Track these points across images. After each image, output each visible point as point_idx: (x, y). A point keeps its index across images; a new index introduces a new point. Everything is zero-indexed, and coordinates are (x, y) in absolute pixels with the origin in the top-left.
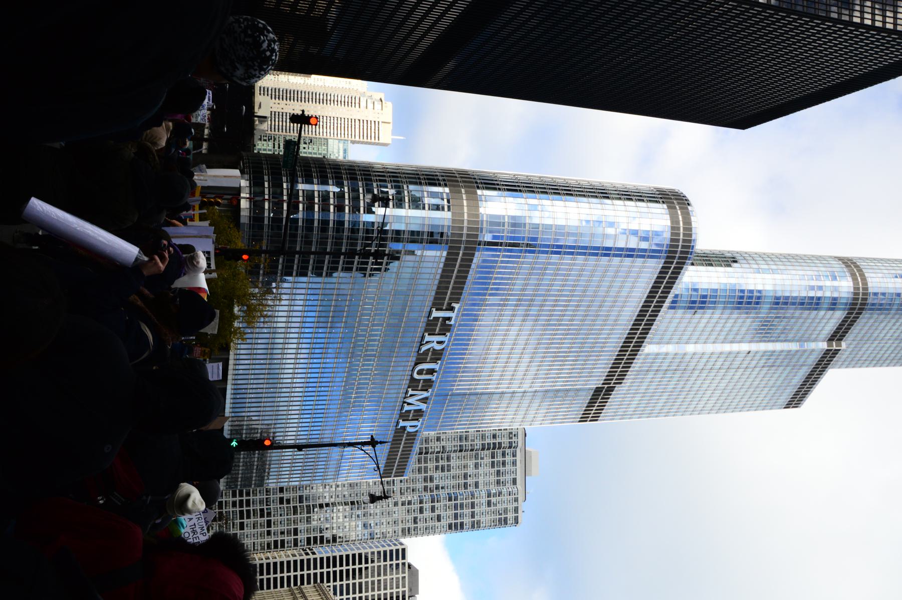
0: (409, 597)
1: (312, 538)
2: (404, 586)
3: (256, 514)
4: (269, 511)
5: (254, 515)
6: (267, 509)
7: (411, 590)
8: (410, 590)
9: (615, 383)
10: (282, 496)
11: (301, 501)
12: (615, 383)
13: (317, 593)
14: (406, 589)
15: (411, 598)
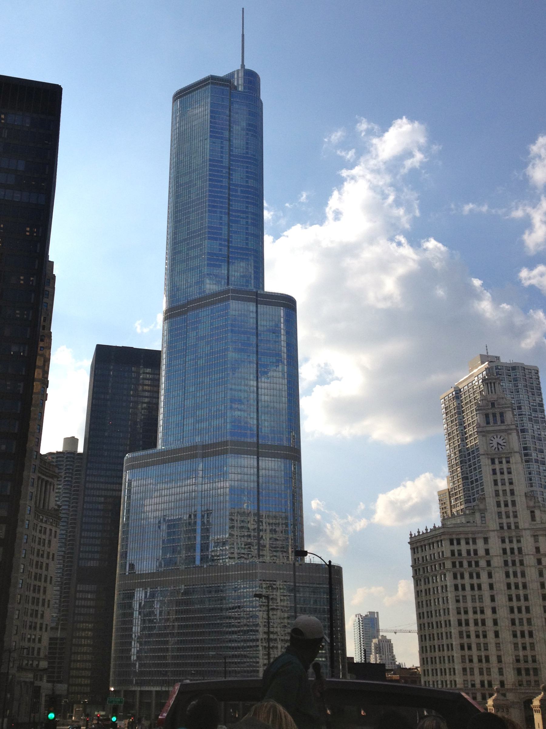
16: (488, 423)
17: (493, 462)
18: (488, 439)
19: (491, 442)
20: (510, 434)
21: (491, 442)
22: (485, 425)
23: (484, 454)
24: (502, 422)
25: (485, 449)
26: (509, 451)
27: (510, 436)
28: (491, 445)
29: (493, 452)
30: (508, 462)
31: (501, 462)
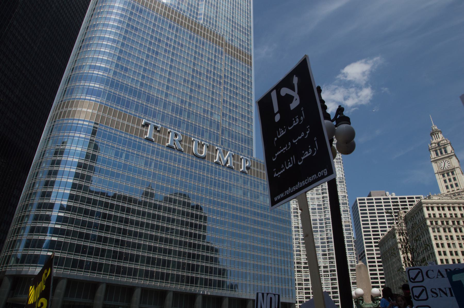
0: (386, 196)
1: (349, 247)
2: (380, 199)
3: (334, 283)
4: (332, 275)
5: (335, 285)
6: (331, 276)
7: (382, 195)
8: (382, 195)
9: (222, 40)
10: (322, 267)
11: (325, 255)
12: (222, 40)
13: (384, 245)
14: (382, 197)
15: (387, 195)
16: (437, 154)
17: (444, 176)
18: (438, 164)
19: (440, 165)
20: (452, 158)
21: (440, 165)
22: (436, 157)
23: (438, 173)
24: (446, 152)
25: (438, 169)
26: (452, 168)
27: (451, 160)
28: (441, 167)
29: (442, 171)
30: (453, 174)
31: (448, 175)
